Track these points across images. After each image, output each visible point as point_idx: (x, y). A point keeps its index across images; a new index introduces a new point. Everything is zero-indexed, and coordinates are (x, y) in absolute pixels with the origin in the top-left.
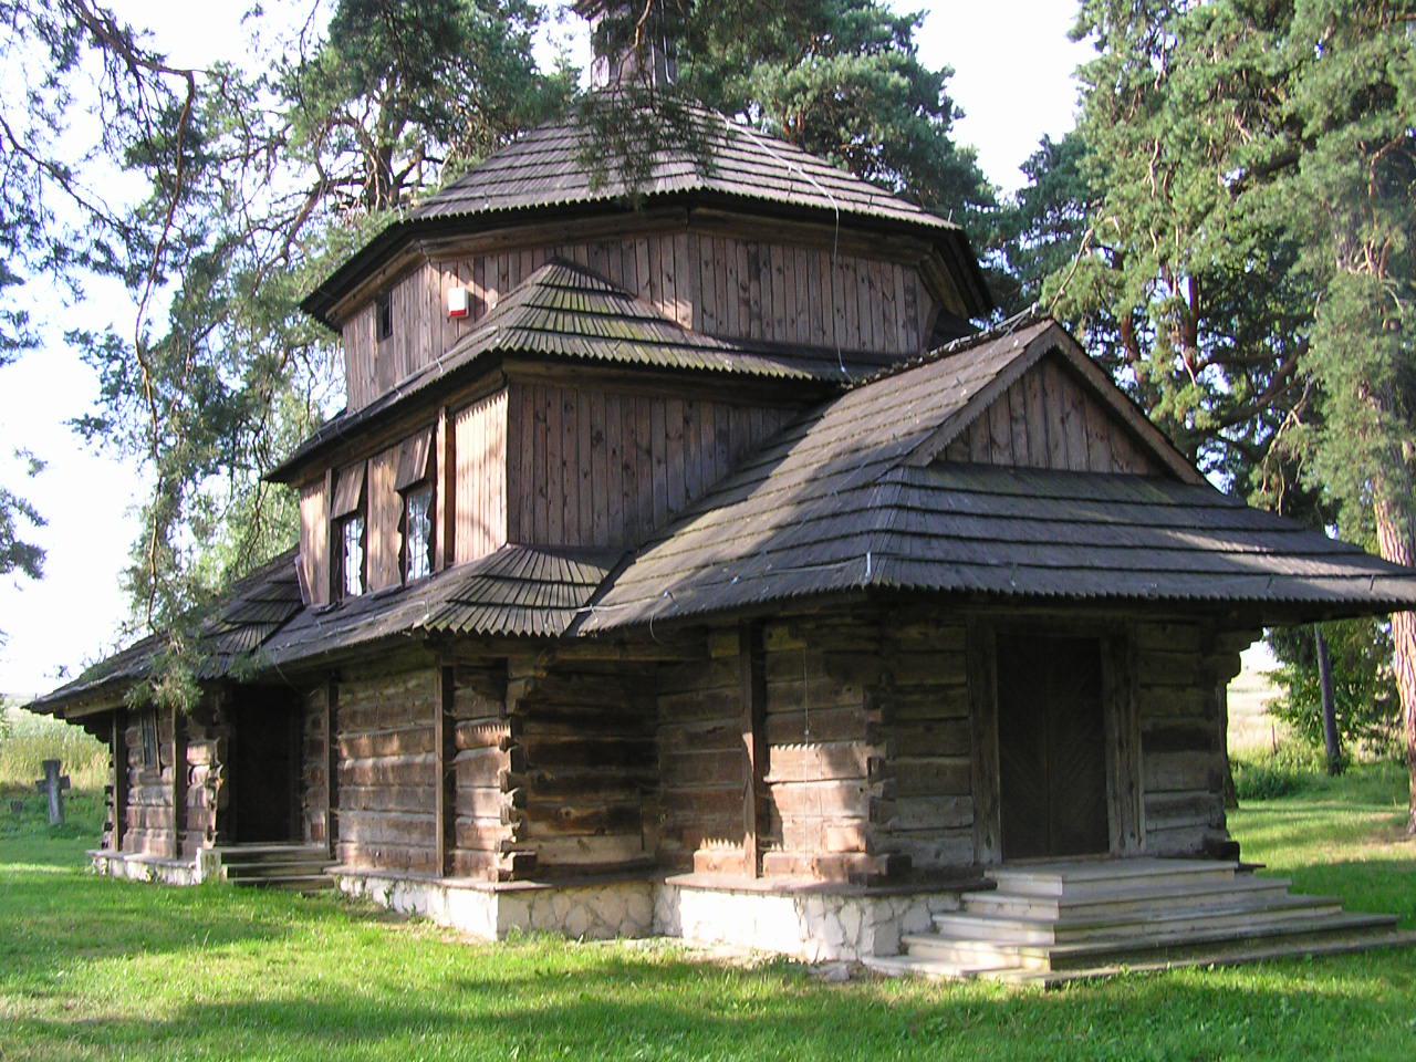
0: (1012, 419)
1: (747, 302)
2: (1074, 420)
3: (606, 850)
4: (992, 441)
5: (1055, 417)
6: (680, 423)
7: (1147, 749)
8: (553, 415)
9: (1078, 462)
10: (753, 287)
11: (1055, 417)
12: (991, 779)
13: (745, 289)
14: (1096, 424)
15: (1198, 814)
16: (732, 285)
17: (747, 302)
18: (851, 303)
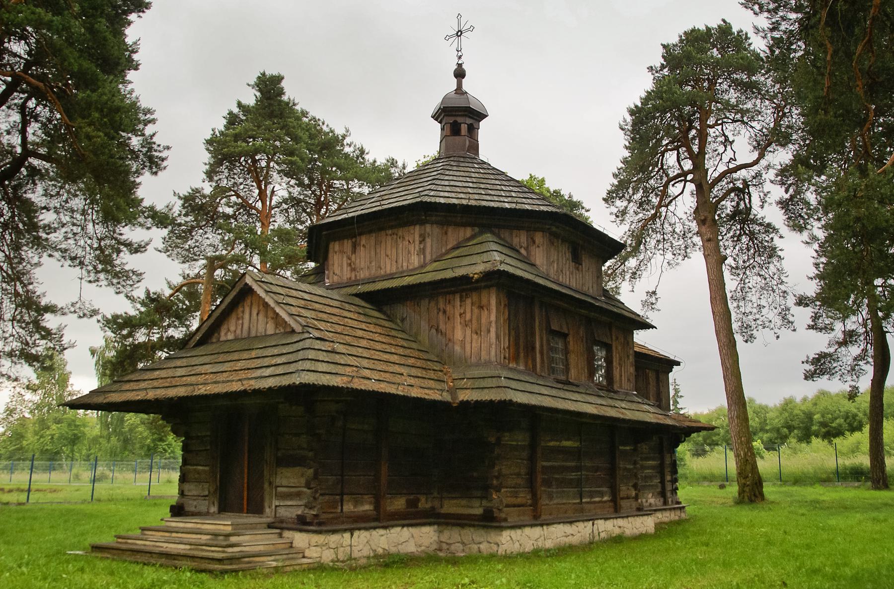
4: (229, 330)
5: (255, 312)
9: (261, 330)
11: (255, 312)
12: (216, 477)
16: (345, 259)
18: (394, 251)
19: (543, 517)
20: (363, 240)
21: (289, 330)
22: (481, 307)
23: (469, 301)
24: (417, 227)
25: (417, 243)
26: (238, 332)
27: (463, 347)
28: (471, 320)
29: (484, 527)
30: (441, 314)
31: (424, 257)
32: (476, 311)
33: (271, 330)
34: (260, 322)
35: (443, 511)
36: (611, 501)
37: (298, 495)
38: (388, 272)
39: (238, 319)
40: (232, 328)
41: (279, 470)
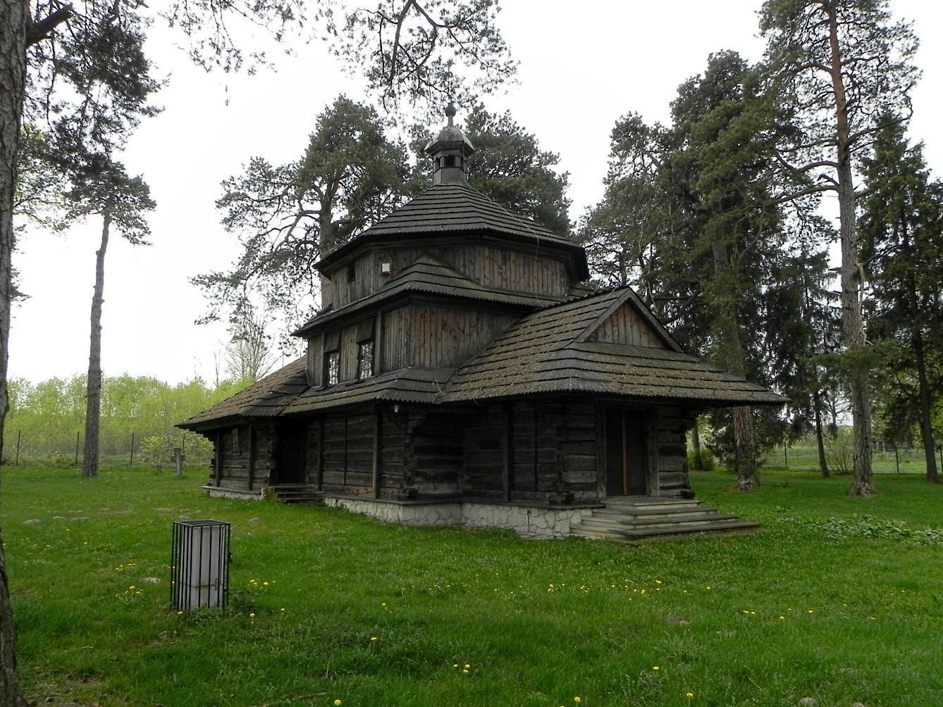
2: (635, 327)
3: (444, 489)
5: (628, 325)
6: (475, 320)
7: (660, 455)
8: (428, 315)
14: (643, 329)
16: (496, 267)
17: (501, 274)
18: (540, 275)
34: (635, 334)
37: (677, 477)
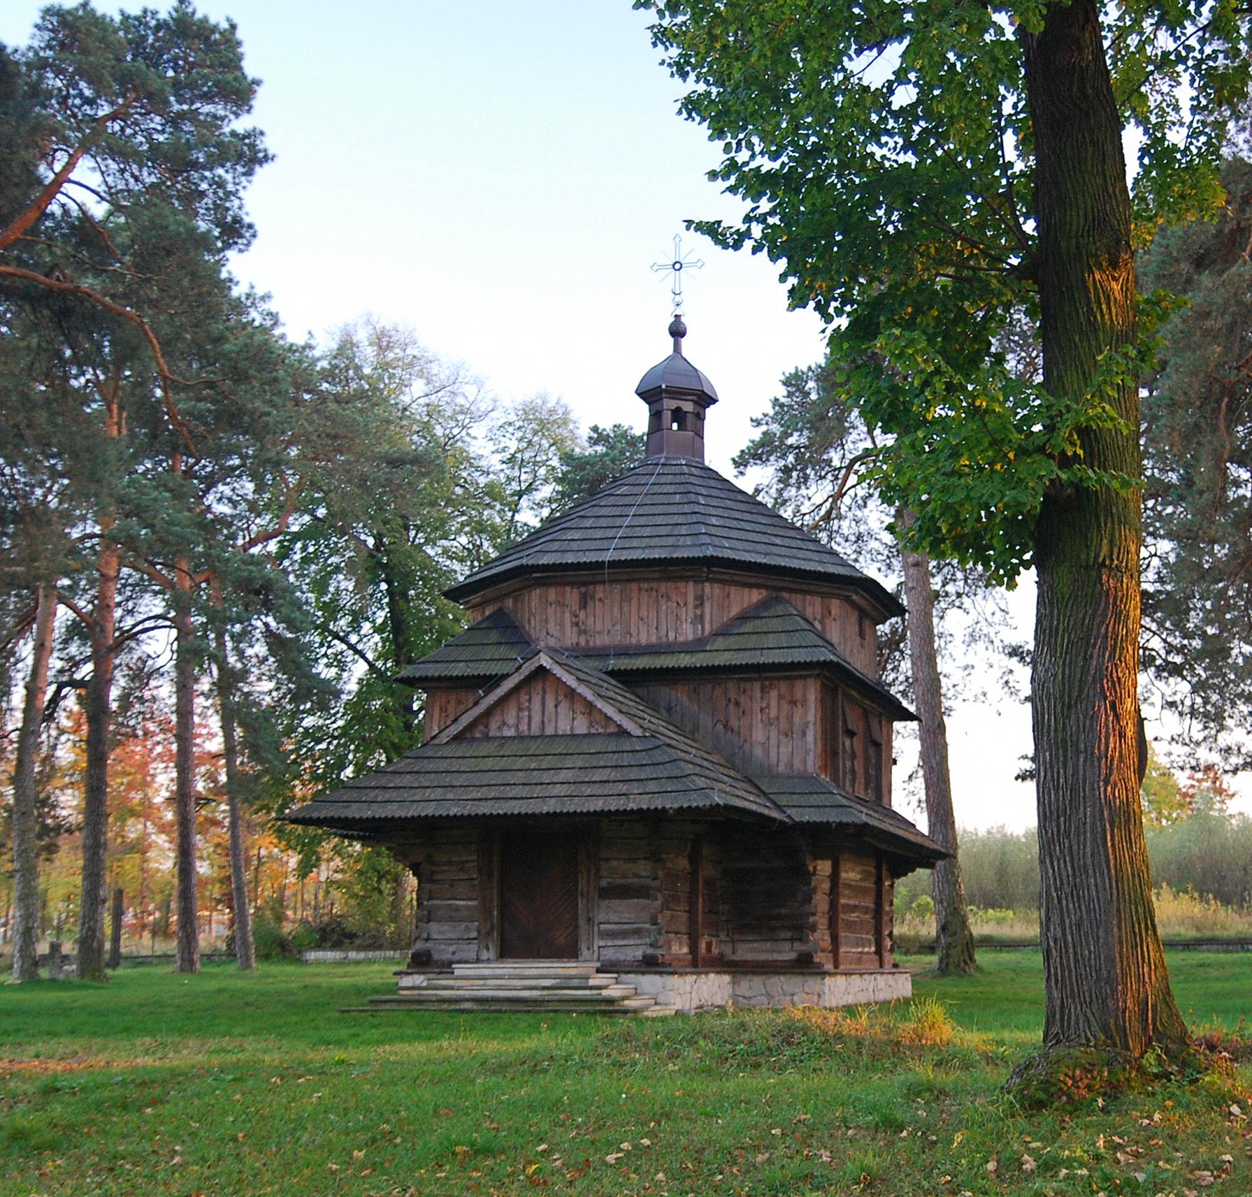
0: (520, 709)
1: (577, 624)
4: (504, 723)
5: (550, 704)
9: (564, 727)
10: (582, 614)
11: (550, 704)
13: (576, 616)
15: (640, 937)
16: (567, 615)
17: (577, 624)
18: (653, 614)
19: (842, 967)
20: (600, 591)
21: (612, 729)
22: (793, 703)
23: (774, 694)
24: (691, 584)
25: (691, 607)
26: (524, 727)
27: (767, 752)
28: (778, 718)
29: (802, 974)
30: (731, 706)
31: (703, 627)
32: (785, 707)
33: (581, 727)
35: (735, 958)
36: (876, 953)
37: (637, 933)
38: (644, 641)
39: (520, 709)
40: (511, 720)
41: (605, 903)
